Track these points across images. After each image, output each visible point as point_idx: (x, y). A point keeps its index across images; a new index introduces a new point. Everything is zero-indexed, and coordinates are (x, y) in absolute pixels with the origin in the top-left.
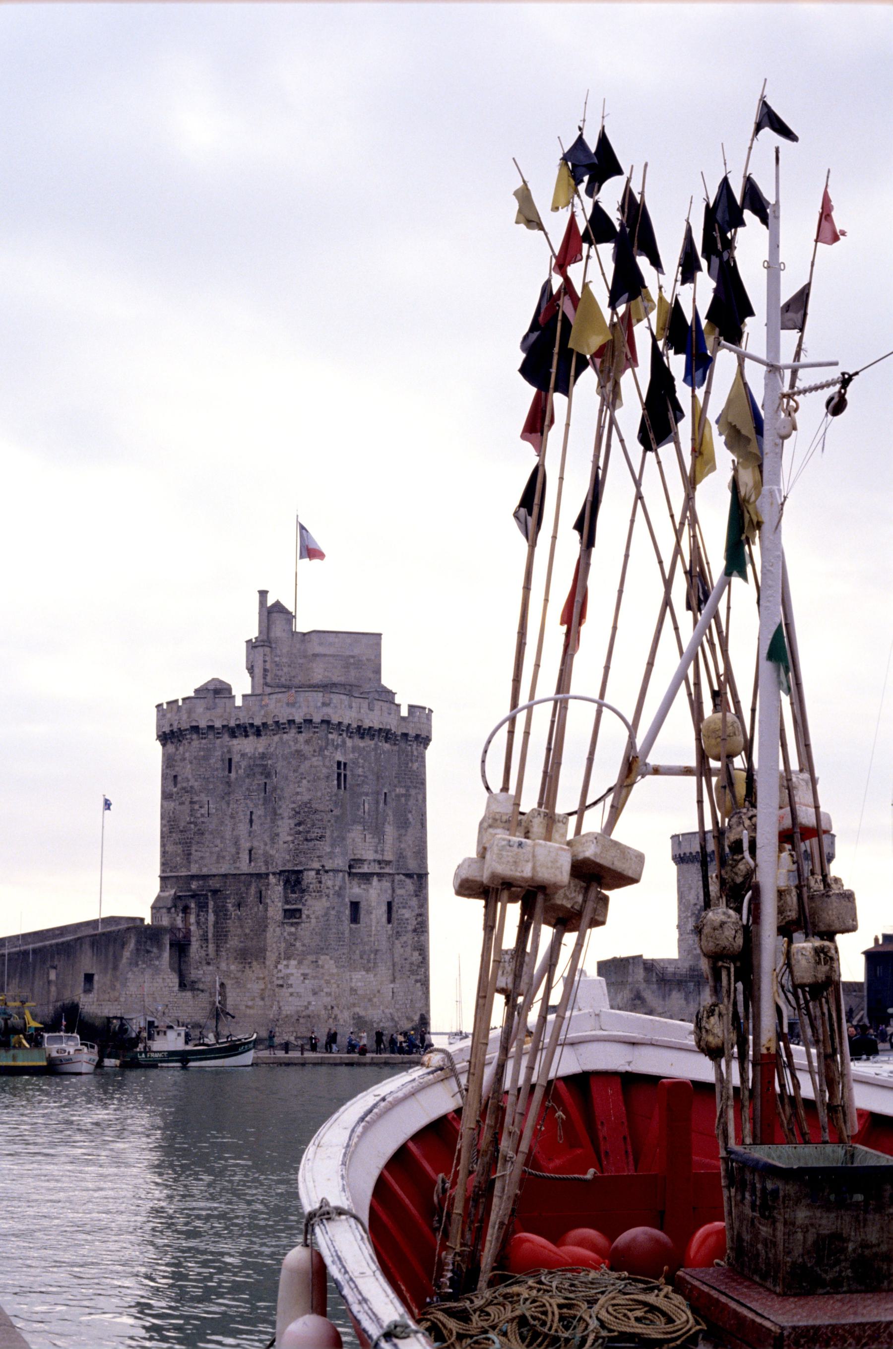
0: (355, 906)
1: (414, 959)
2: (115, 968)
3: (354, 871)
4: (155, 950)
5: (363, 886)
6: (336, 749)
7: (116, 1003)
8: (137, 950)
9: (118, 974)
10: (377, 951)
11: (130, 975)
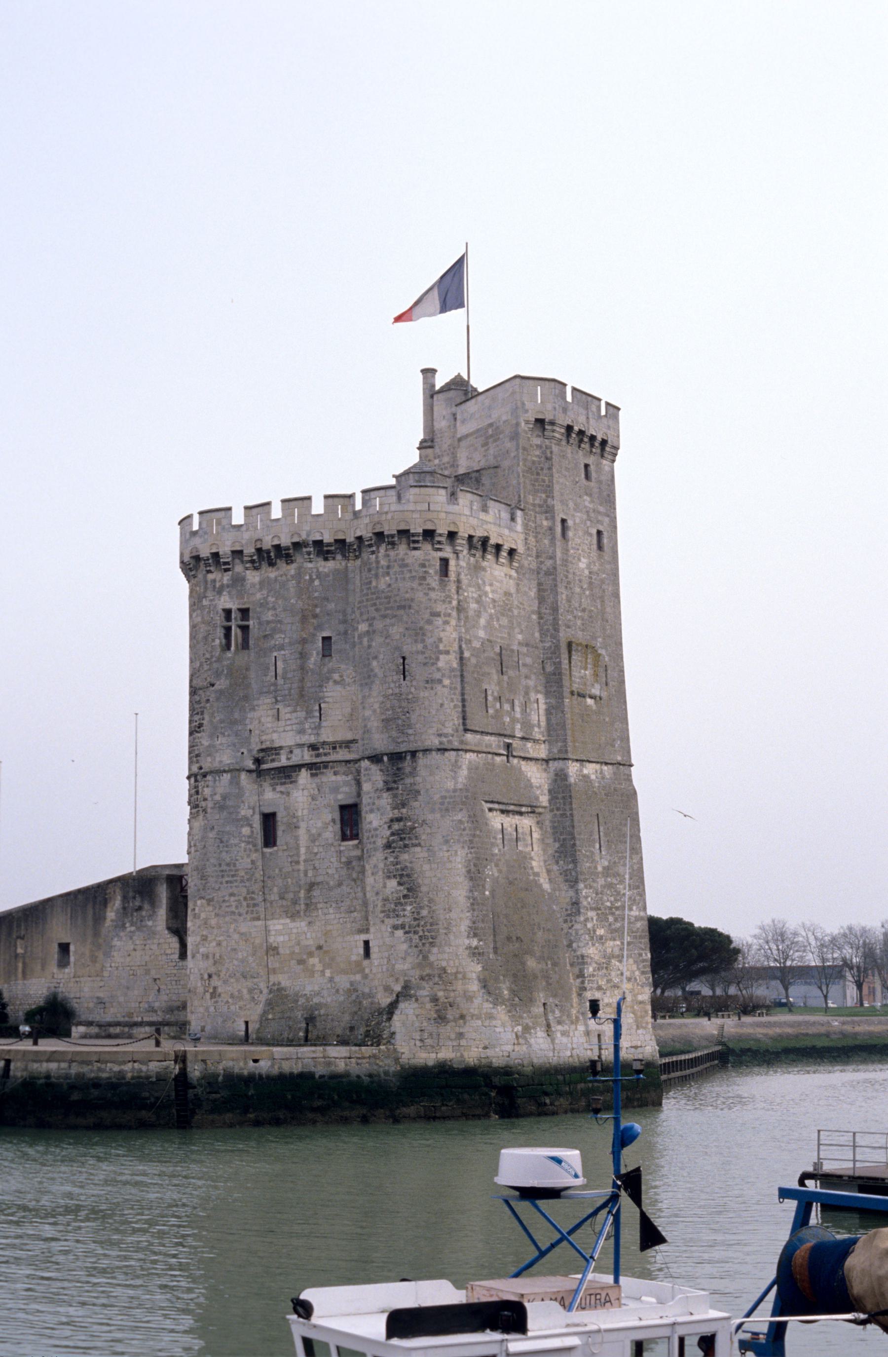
0: (269, 820)
1: (388, 891)
2: (96, 934)
3: (264, 767)
4: (146, 906)
5: (279, 788)
6: (220, 592)
7: (99, 979)
8: (124, 908)
9: (101, 941)
10: (312, 886)
11: (116, 942)
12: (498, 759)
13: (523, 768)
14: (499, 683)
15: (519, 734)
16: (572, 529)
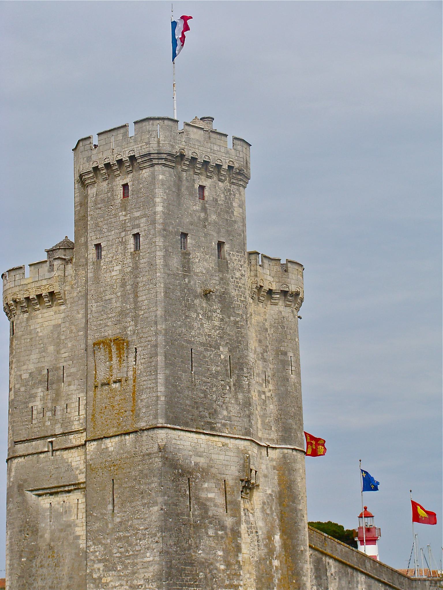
12: (42, 456)
13: (65, 456)
14: (43, 399)
15: (58, 431)
16: (106, 248)
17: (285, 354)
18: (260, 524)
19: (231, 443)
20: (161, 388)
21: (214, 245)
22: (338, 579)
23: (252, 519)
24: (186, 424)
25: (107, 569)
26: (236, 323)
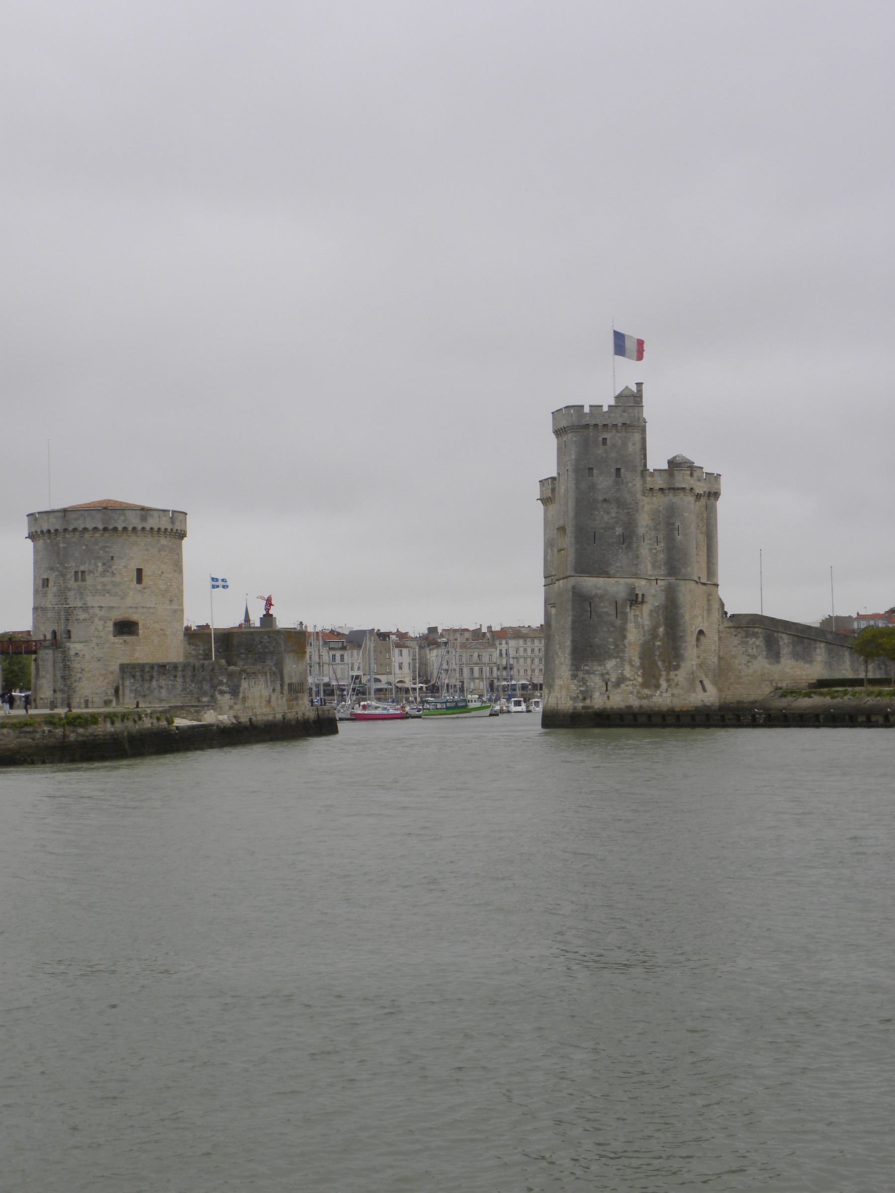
17: (673, 524)
18: (647, 622)
19: (622, 581)
20: (573, 555)
21: (613, 471)
22: (791, 647)
23: (640, 620)
24: (589, 573)
25: (560, 648)
26: (628, 513)
